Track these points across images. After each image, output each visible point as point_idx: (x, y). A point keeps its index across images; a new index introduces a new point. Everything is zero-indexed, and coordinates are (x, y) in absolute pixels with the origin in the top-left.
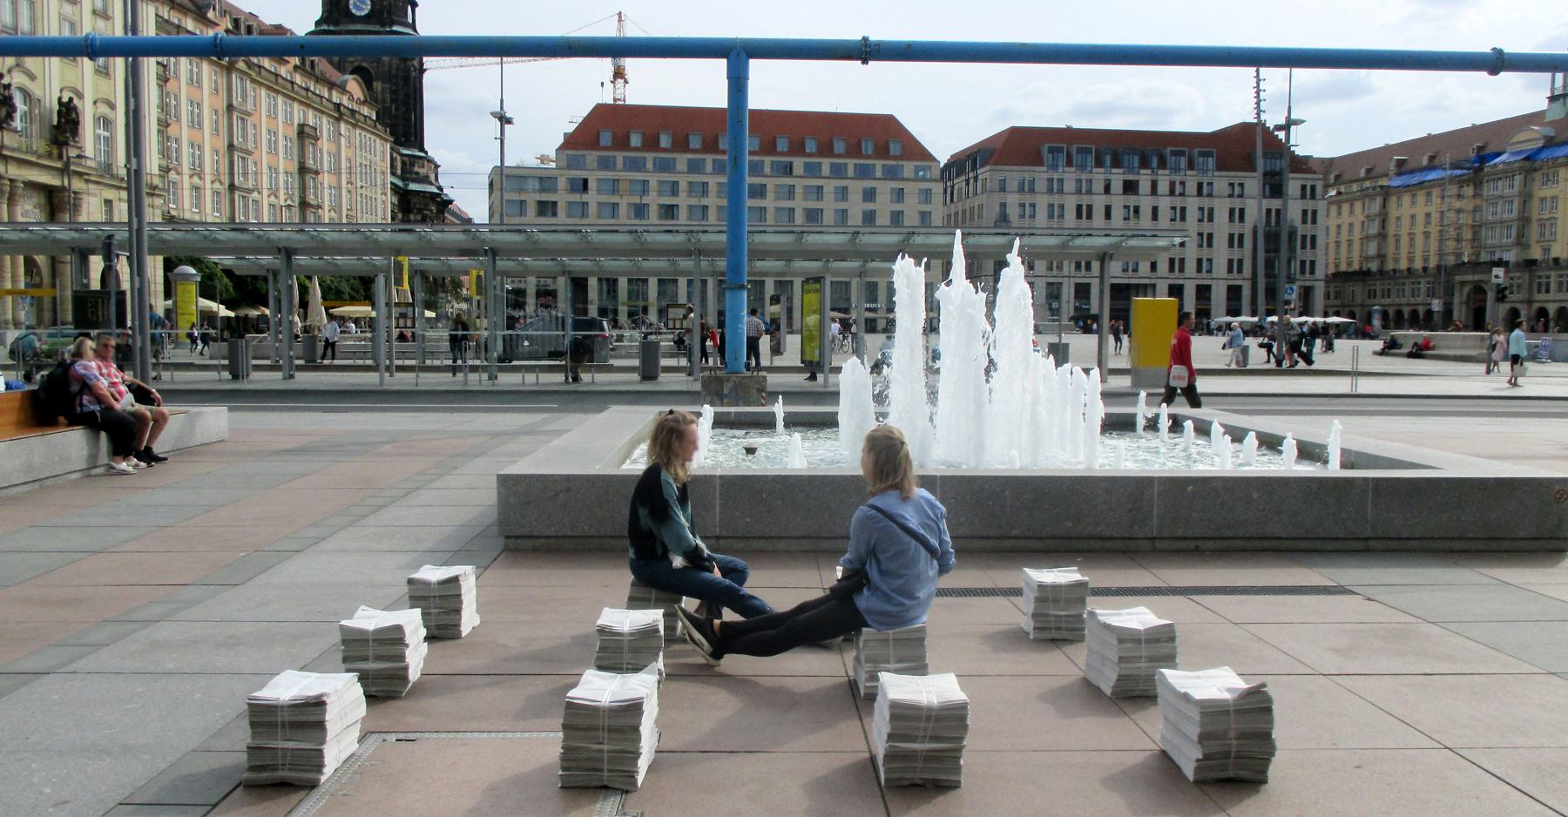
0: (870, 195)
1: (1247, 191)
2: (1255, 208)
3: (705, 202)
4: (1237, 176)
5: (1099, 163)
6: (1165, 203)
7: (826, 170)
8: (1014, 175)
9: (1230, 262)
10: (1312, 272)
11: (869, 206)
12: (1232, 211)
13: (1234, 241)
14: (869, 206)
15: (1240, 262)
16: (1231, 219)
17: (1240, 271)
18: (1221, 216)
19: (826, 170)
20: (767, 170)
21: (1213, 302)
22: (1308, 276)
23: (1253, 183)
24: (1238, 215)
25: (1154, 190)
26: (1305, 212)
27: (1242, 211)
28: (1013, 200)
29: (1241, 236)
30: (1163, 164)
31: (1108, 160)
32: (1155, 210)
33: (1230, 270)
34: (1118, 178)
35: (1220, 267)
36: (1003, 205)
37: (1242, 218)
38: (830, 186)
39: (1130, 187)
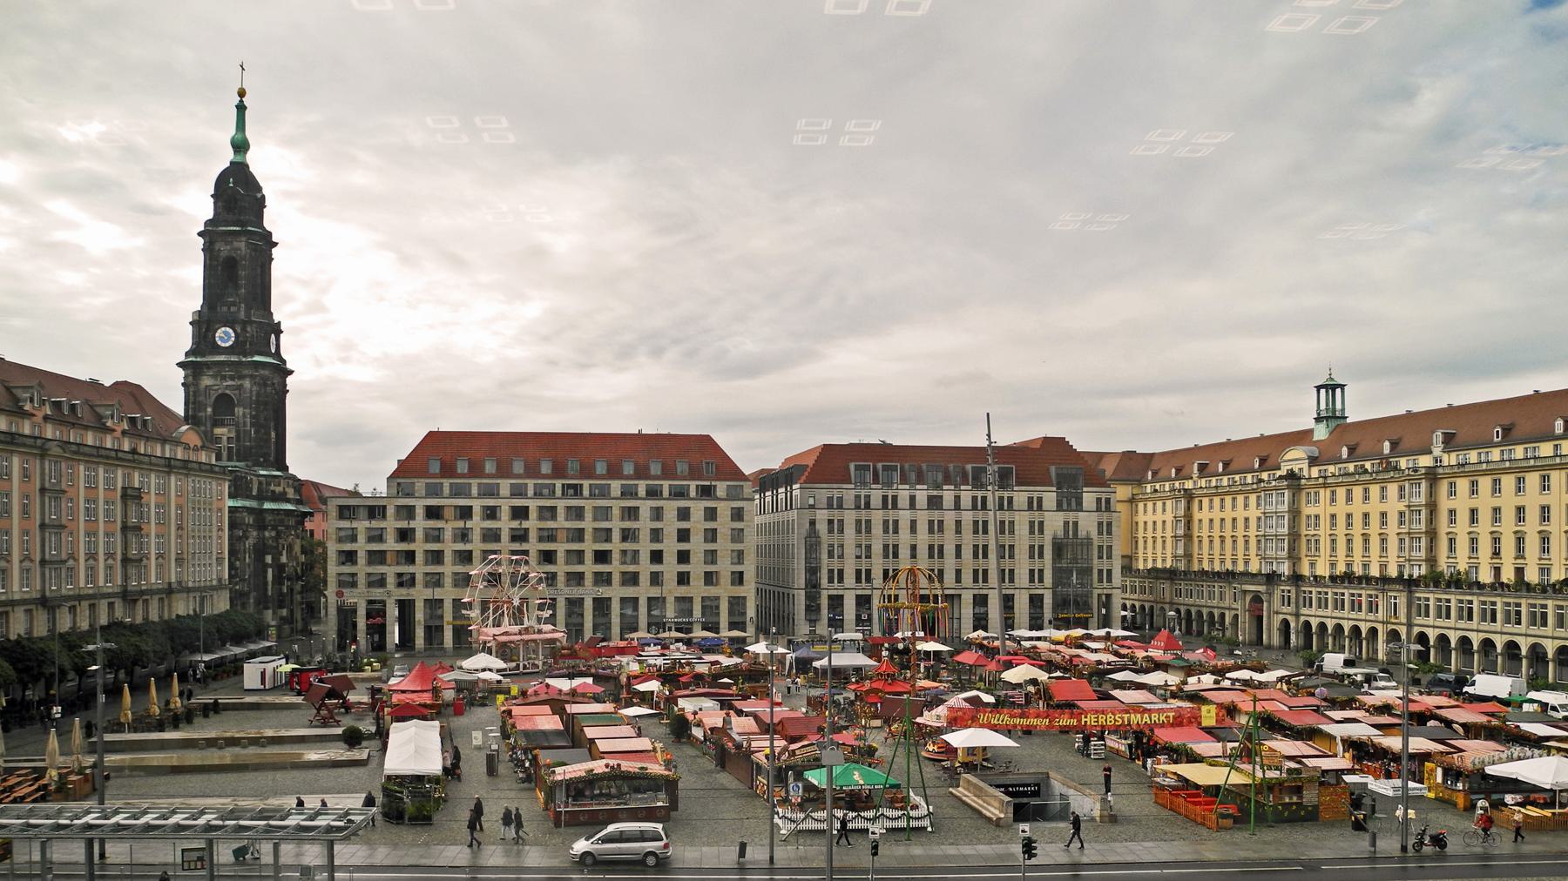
0: (684, 514)
1: (1045, 505)
2: (1054, 522)
4: (1036, 491)
5: (904, 480)
6: (967, 517)
8: (823, 493)
9: (1032, 572)
10: (1109, 580)
12: (1032, 524)
13: (1036, 552)
15: (1041, 571)
16: (1032, 532)
17: (1041, 580)
18: (1022, 529)
19: (642, 492)
21: (1016, 610)
23: (1050, 497)
24: (1037, 528)
25: (957, 507)
26: (1100, 524)
27: (1041, 524)
28: (822, 516)
29: (1041, 547)
31: (913, 476)
32: (958, 523)
33: (1032, 580)
35: (1022, 578)
36: (813, 523)
37: (1041, 531)
38: (645, 507)
39: (935, 503)
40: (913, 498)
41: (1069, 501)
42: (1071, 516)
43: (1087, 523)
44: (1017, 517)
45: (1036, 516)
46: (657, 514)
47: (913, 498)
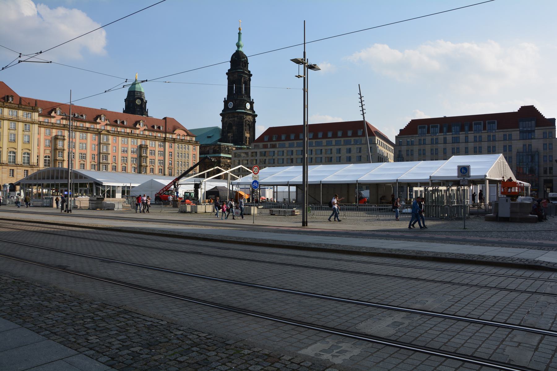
1: (513, 138)
3: (292, 157)
4: (508, 132)
5: (441, 131)
7: (334, 143)
11: (349, 155)
14: (349, 155)
19: (334, 143)
20: (314, 144)
22: (548, 175)
25: (467, 141)
30: (470, 129)
34: (449, 137)
36: (400, 151)
37: (510, 150)
38: (335, 148)
40: (445, 139)
41: (527, 134)
42: (527, 142)
43: (537, 144)
44: (497, 144)
45: (507, 143)
46: (339, 151)
47: (445, 139)
